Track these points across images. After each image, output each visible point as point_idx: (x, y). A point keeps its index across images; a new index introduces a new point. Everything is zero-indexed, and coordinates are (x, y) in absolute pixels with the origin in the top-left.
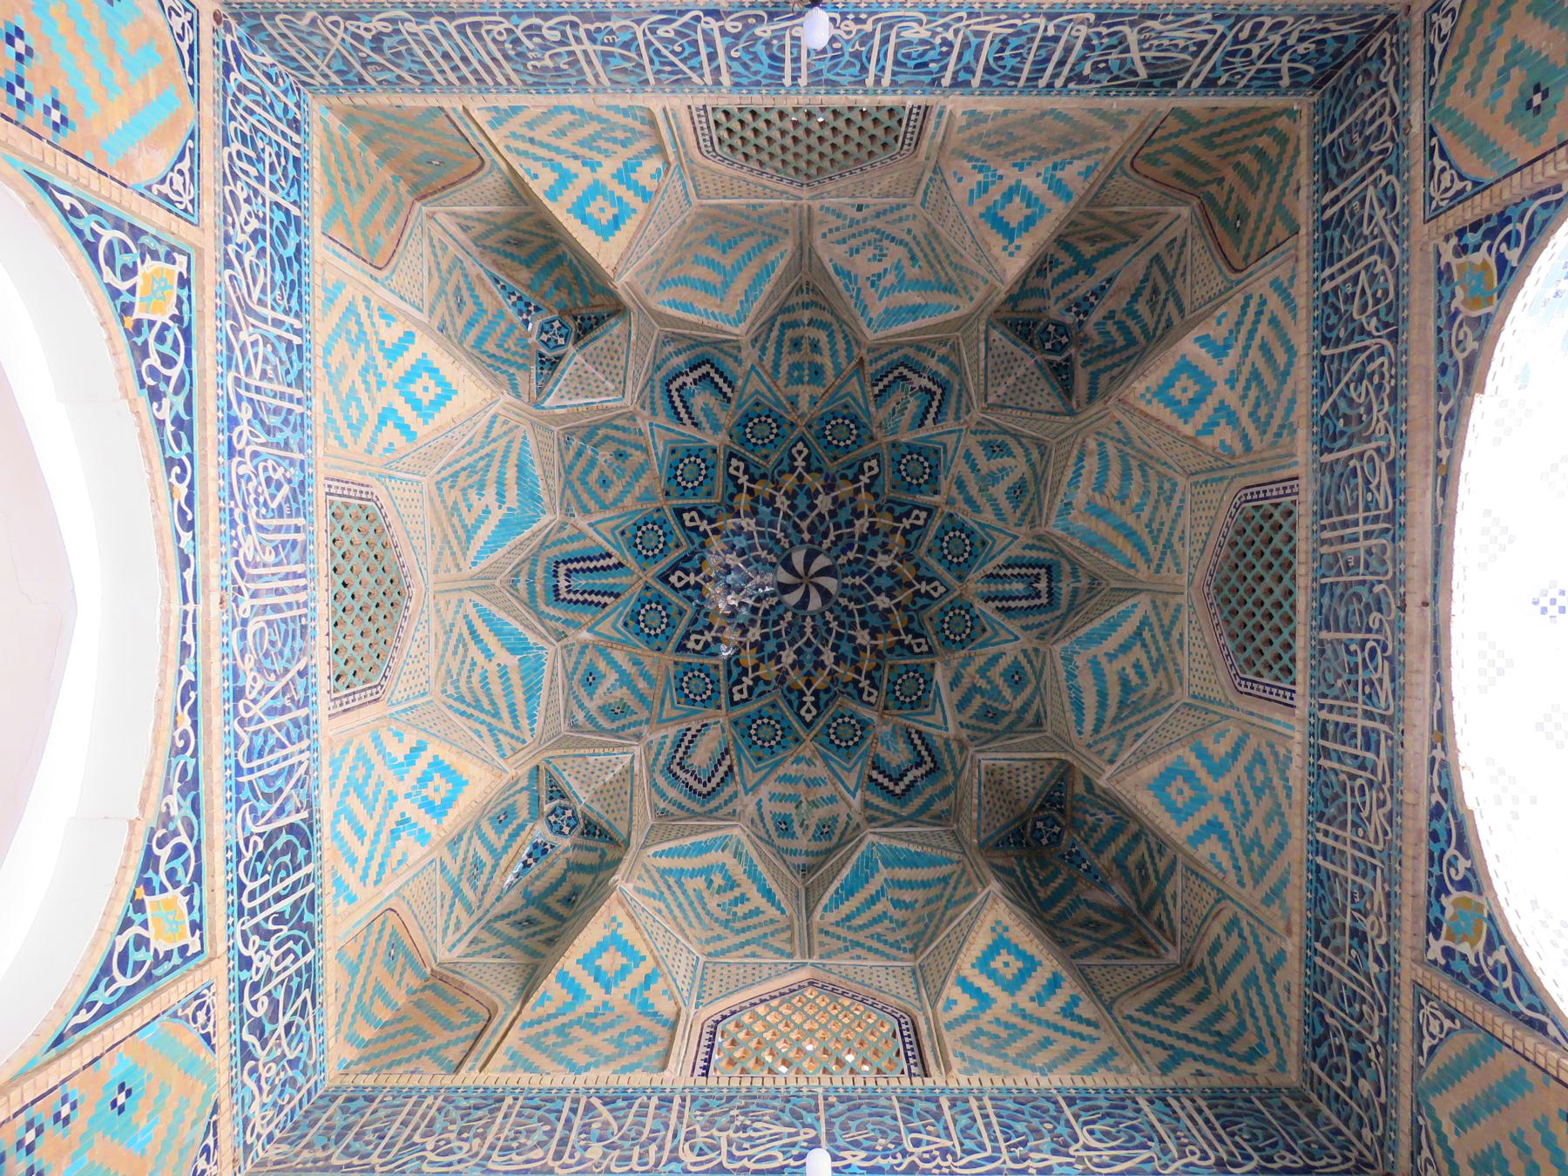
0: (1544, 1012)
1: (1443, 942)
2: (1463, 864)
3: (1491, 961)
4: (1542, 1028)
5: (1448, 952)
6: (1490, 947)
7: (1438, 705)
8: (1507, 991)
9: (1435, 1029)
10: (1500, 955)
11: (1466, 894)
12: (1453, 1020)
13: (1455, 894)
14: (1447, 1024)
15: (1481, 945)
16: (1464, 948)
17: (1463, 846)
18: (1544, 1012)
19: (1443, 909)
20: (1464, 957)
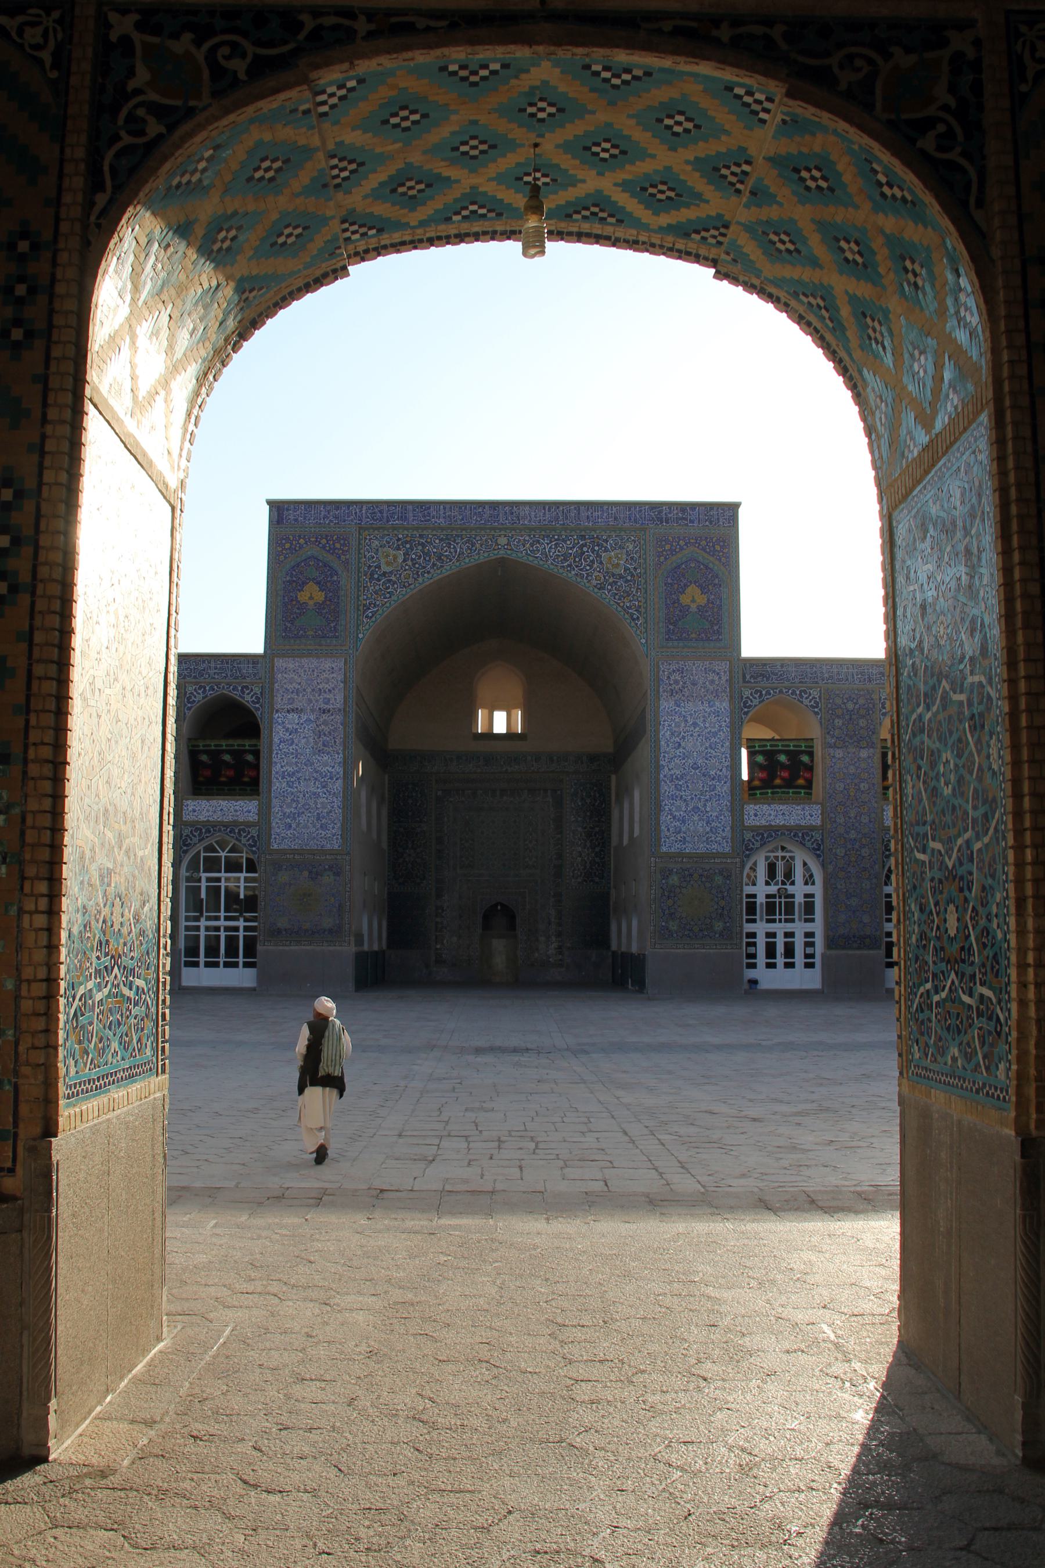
0: (117, 188)
1: (137, 37)
2: (239, 66)
3: (141, 112)
4: (97, 186)
5: (126, 42)
6: (159, 111)
7: (421, 23)
8: (116, 138)
9: (33, 36)
10: (154, 128)
11: (206, 74)
12: (55, 66)
13: (200, 55)
14: (46, 56)
15: (153, 96)
16: (142, 76)
17: (261, 68)
18: (117, 188)
19: (176, 36)
20: (131, 73)
